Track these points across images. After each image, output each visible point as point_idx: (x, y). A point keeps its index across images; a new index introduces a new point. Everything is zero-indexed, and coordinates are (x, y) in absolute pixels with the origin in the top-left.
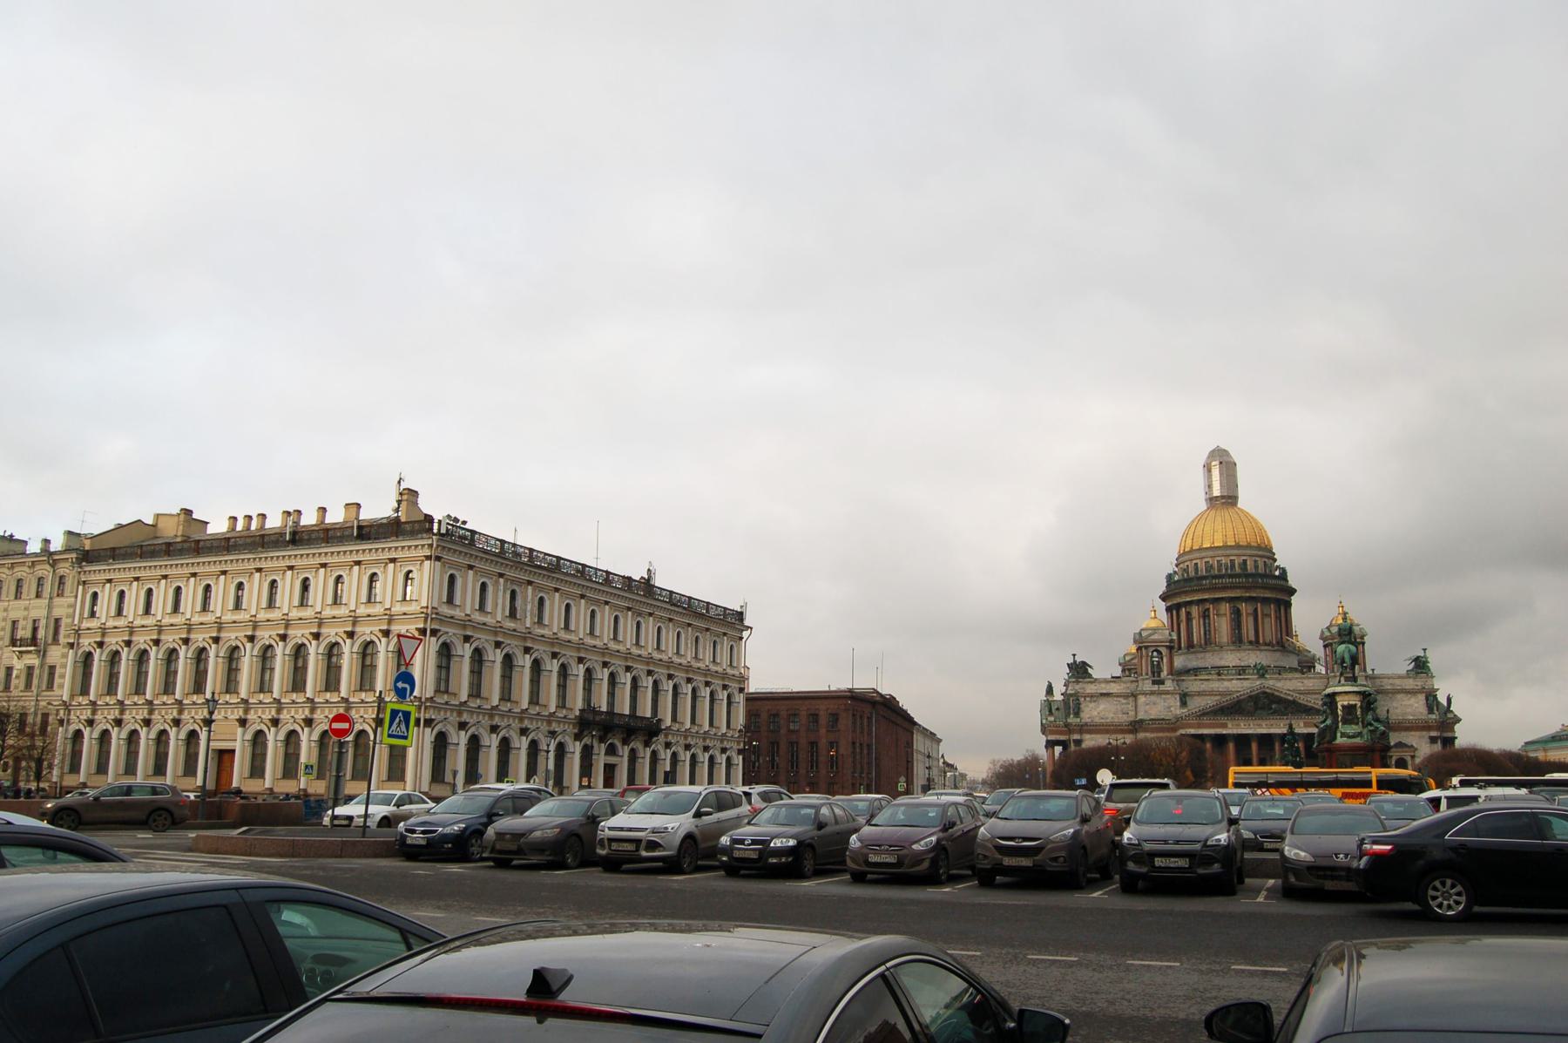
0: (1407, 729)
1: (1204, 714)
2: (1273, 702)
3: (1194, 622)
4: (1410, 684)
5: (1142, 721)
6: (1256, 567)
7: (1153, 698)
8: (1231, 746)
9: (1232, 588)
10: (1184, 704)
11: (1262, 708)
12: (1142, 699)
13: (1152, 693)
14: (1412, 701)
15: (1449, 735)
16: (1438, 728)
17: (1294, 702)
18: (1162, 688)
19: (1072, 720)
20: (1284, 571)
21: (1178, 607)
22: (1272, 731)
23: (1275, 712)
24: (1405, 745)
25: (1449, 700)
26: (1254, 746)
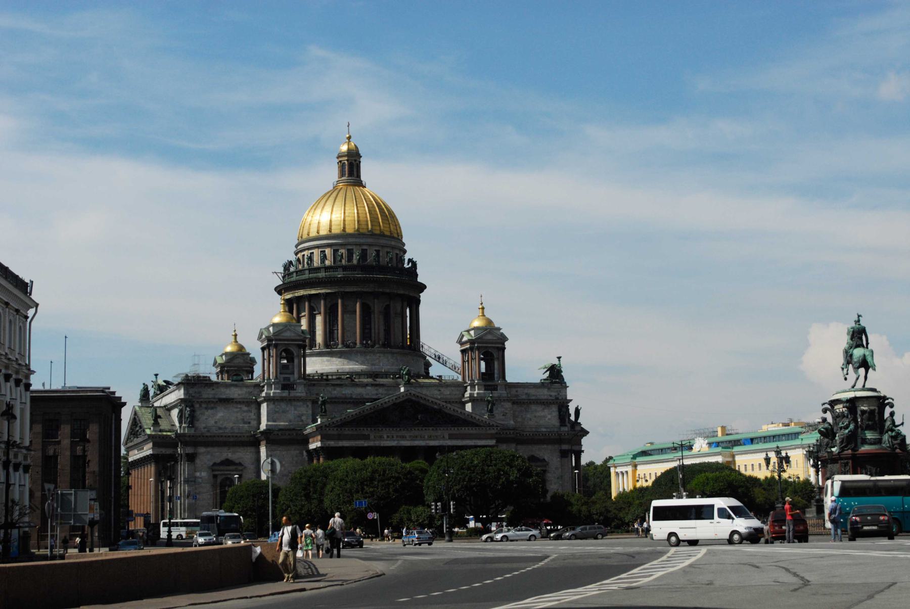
1: (344, 424)
3: (319, 320)
4: (544, 394)
7: (283, 406)
14: (546, 412)
15: (576, 448)
16: (569, 441)
18: (293, 394)
20: (414, 265)
21: (299, 300)
25: (577, 412)
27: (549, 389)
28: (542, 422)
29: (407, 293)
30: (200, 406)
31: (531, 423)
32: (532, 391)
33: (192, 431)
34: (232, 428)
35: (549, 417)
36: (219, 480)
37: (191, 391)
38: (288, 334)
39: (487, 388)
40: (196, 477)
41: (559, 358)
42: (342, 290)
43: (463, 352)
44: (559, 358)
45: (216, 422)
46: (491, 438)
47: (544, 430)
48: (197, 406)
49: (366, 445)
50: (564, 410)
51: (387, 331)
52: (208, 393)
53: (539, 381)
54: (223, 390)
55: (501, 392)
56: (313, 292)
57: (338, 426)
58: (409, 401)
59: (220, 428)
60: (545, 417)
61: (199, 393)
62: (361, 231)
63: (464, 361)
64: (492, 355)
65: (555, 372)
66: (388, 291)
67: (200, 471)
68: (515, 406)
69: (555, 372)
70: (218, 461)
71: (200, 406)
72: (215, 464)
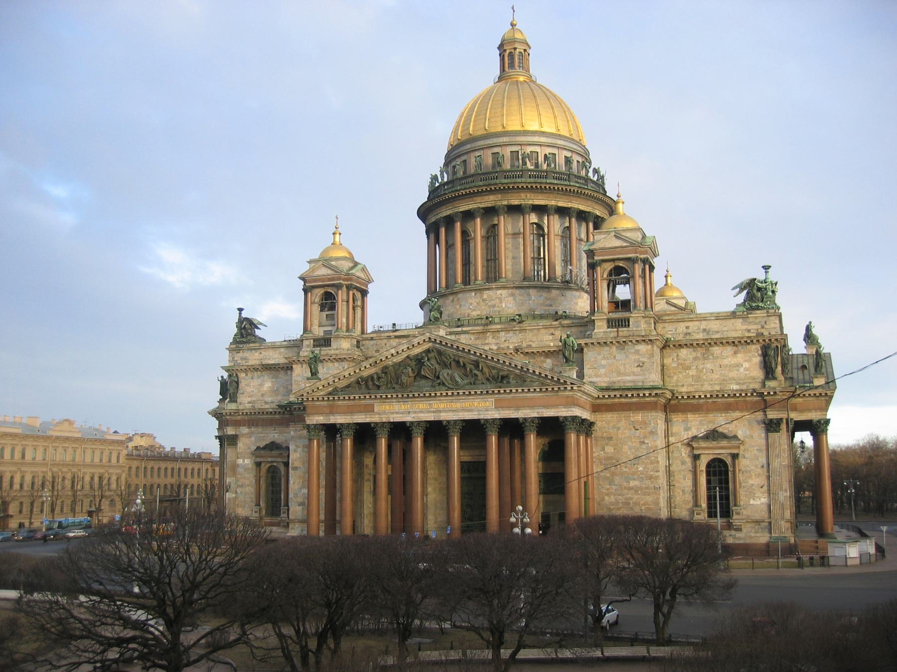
0: (728, 408)
1: (335, 392)
4: (738, 329)
10: (314, 374)
14: (740, 357)
17: (476, 364)
22: (444, 417)
24: (724, 436)
27: (744, 318)
28: (731, 375)
29: (553, 203)
31: (715, 376)
32: (714, 325)
33: (232, 406)
35: (746, 365)
36: (264, 468)
37: (238, 356)
38: (323, 271)
41: (766, 268)
47: (735, 387)
48: (242, 375)
49: (368, 420)
52: (254, 358)
53: (732, 308)
54: (271, 353)
57: (330, 394)
59: (266, 403)
60: (738, 365)
65: (757, 295)
66: (516, 202)
69: (757, 295)
70: (262, 444)
72: (258, 448)
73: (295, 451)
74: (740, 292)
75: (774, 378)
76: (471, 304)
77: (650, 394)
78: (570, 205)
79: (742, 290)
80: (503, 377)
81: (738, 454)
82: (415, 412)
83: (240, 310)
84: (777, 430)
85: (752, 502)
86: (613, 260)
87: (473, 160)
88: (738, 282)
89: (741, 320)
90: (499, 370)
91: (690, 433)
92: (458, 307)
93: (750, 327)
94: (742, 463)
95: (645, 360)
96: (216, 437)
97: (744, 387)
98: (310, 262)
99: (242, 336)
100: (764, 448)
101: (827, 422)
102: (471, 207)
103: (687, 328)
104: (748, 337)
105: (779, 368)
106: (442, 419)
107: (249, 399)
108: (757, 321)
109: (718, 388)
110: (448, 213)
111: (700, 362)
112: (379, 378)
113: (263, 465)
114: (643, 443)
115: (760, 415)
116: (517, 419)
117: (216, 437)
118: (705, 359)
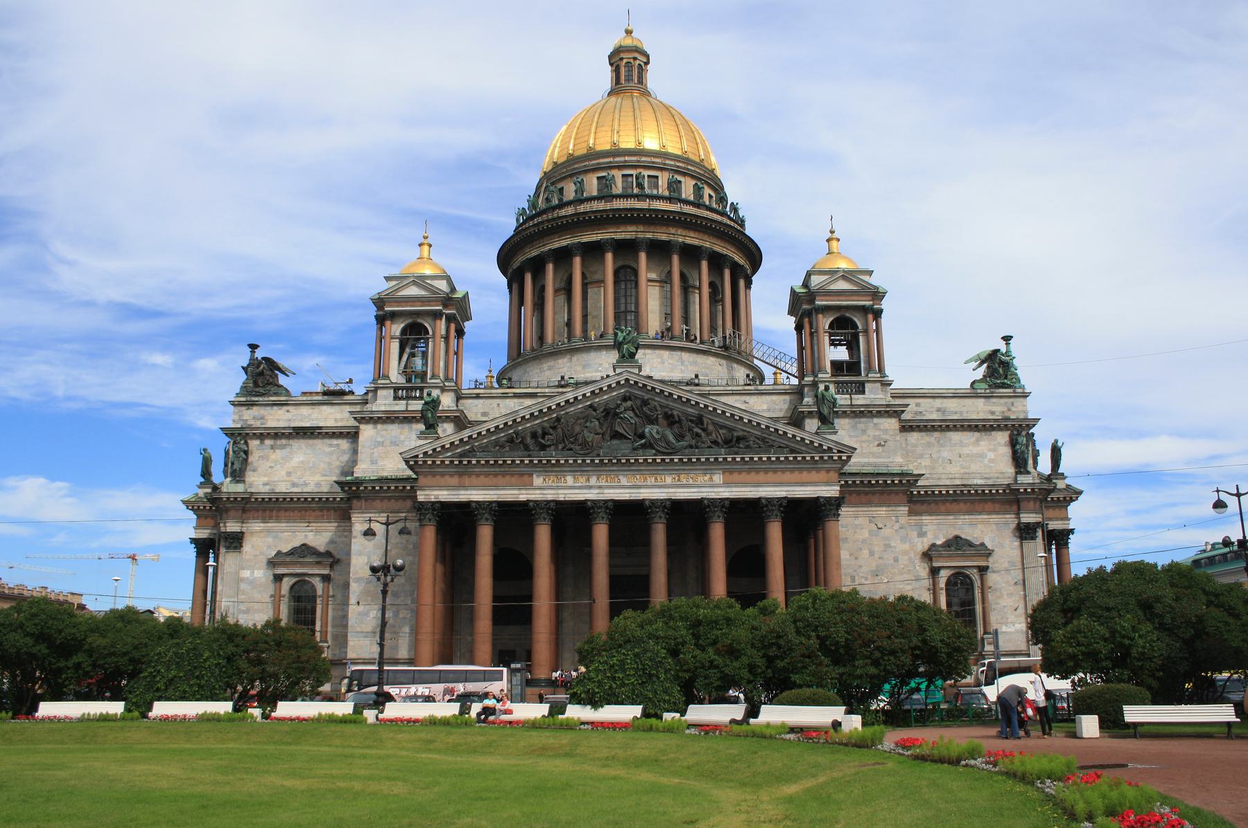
2: (652, 421)
4: (978, 409)
5: (358, 482)
6: (674, 186)
7: (393, 430)
8: (543, 535)
9: (619, 232)
10: (431, 427)
11: (617, 436)
12: (367, 432)
13: (389, 418)
15: (1054, 525)
17: (699, 420)
19: (230, 487)
20: (735, 208)
23: (648, 446)
24: (970, 544)
25: (1056, 453)
26: (601, 534)
28: (974, 467)
29: (707, 245)
30: (262, 443)
33: (240, 488)
34: (318, 484)
35: (991, 455)
36: (287, 583)
38: (413, 291)
39: (842, 387)
40: (240, 580)
41: (1007, 339)
42: (576, 240)
43: (799, 328)
44: (1007, 339)
45: (289, 474)
46: (827, 483)
50: (1023, 440)
51: (668, 316)
54: (305, 411)
55: (873, 395)
56: (534, 253)
57: (462, 455)
58: (625, 398)
59: (294, 485)
60: (982, 456)
61: (262, 418)
62: (623, 146)
63: (801, 349)
64: (855, 326)
65: (998, 370)
66: (664, 237)
67: (252, 568)
68: (914, 437)
69: (998, 370)
70: (286, 548)
71: (262, 443)
72: (279, 553)
73: (360, 554)
74: (980, 365)
75: (1028, 473)
76: (601, 365)
77: (900, 481)
78: (725, 252)
79: (983, 362)
80: (739, 439)
81: (987, 568)
82: (600, 487)
83: (253, 347)
84: (1034, 538)
85: (1004, 629)
86: (839, 308)
87: (595, 182)
88: (974, 354)
89: (983, 400)
90: (731, 430)
91: (925, 540)
92: (579, 368)
93: (994, 409)
94: (992, 578)
95: (887, 437)
96: (193, 541)
97: (990, 482)
98: (388, 279)
99: (256, 384)
100: (1019, 559)
101: (1072, 531)
102: (599, 237)
103: (917, 405)
104: (995, 420)
105: (1030, 462)
106: (641, 497)
107: (266, 479)
108: (1003, 401)
109: (958, 482)
110: (564, 243)
111: (936, 449)
112: (544, 434)
113: (285, 580)
114: (888, 546)
115: (1010, 520)
116: (760, 499)
117: (193, 541)
118: (942, 446)
